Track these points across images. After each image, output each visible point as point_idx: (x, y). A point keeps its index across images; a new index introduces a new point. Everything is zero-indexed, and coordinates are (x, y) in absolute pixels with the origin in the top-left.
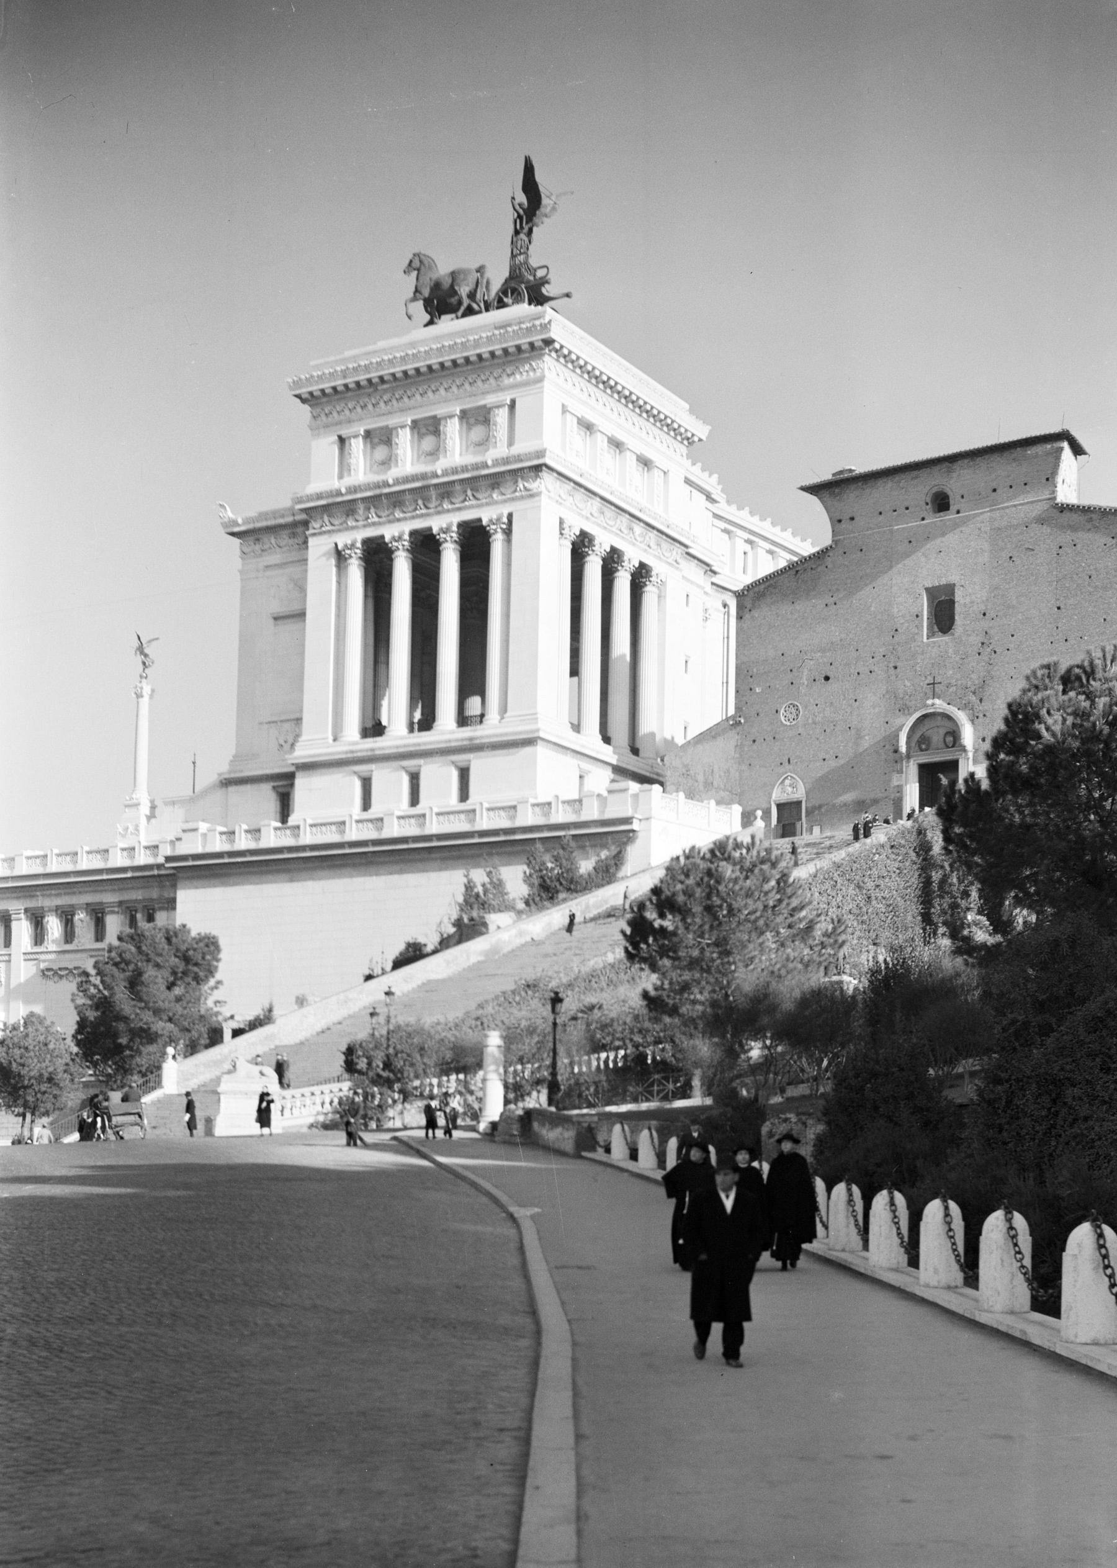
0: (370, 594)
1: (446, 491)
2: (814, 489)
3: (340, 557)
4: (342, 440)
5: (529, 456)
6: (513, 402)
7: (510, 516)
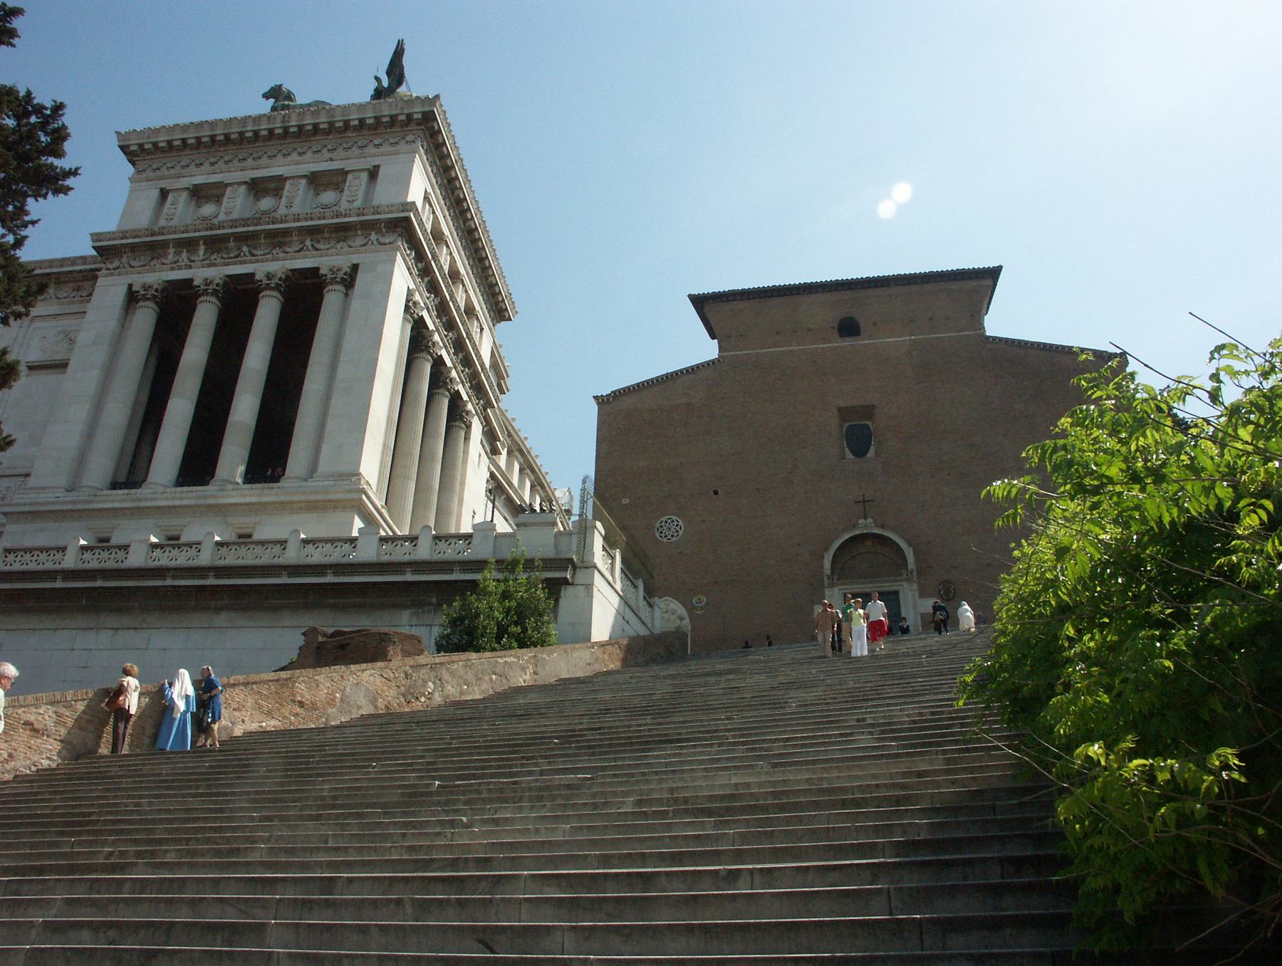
0: (153, 361)
1: (278, 239)
2: (701, 303)
3: (132, 298)
4: (164, 194)
5: (391, 208)
6: (377, 168)
7: (355, 268)
